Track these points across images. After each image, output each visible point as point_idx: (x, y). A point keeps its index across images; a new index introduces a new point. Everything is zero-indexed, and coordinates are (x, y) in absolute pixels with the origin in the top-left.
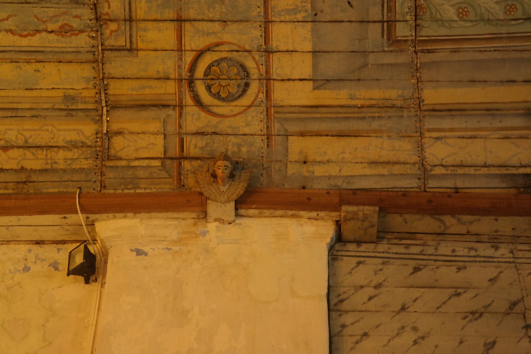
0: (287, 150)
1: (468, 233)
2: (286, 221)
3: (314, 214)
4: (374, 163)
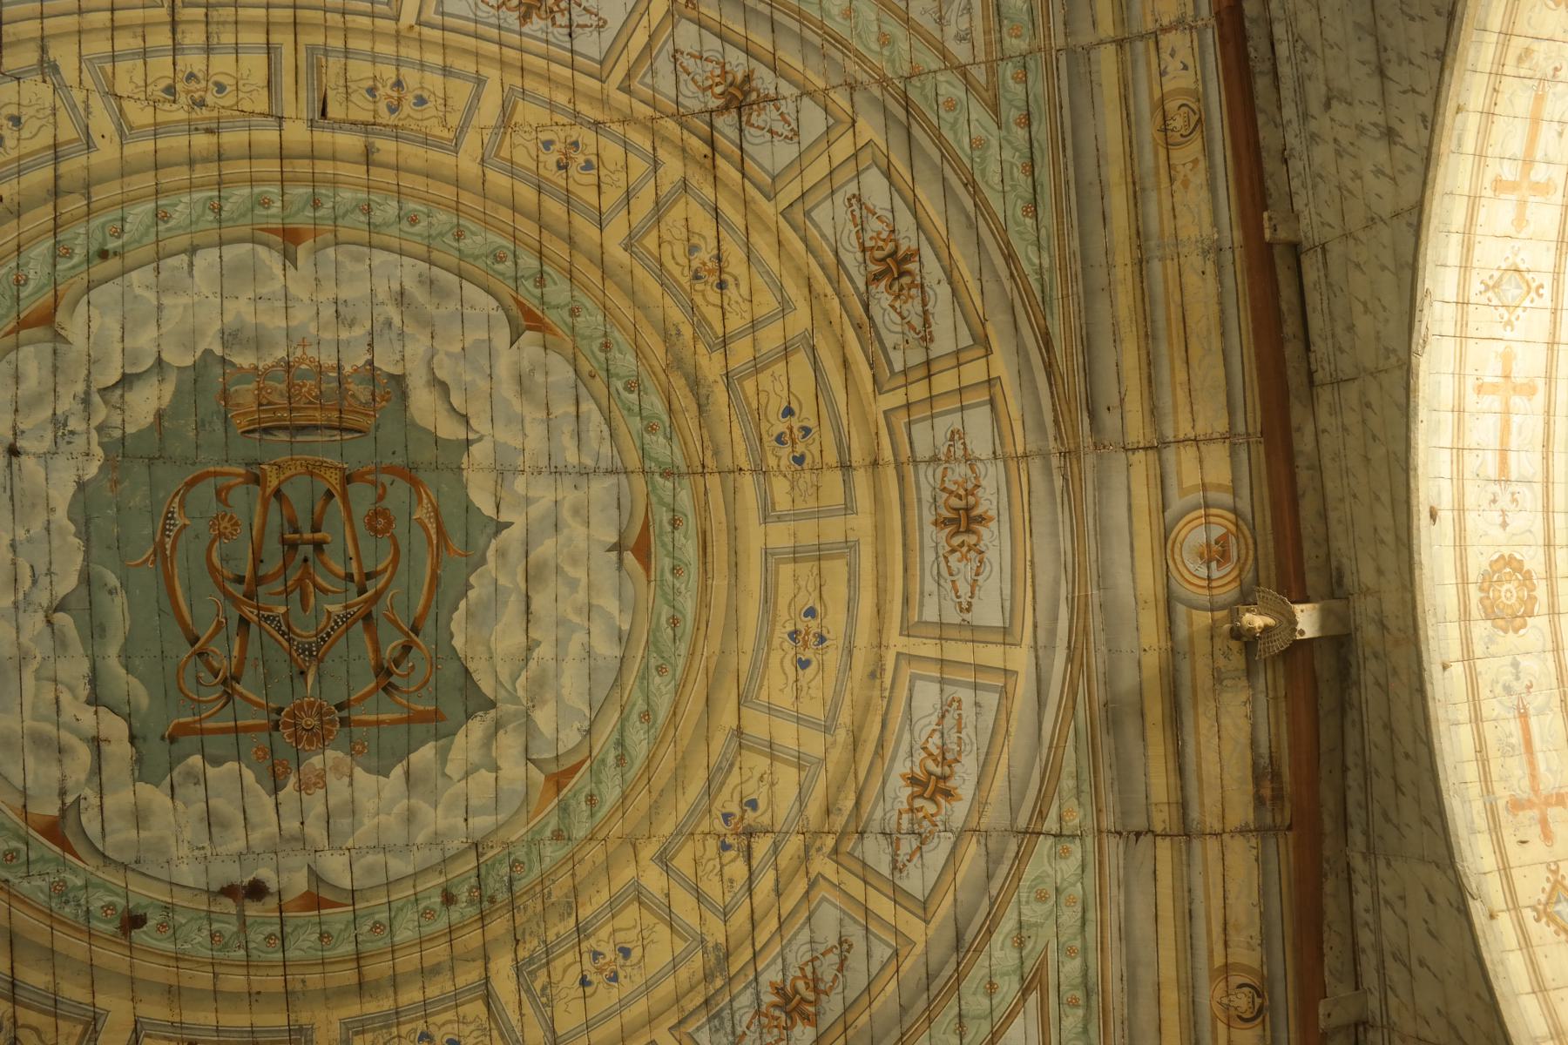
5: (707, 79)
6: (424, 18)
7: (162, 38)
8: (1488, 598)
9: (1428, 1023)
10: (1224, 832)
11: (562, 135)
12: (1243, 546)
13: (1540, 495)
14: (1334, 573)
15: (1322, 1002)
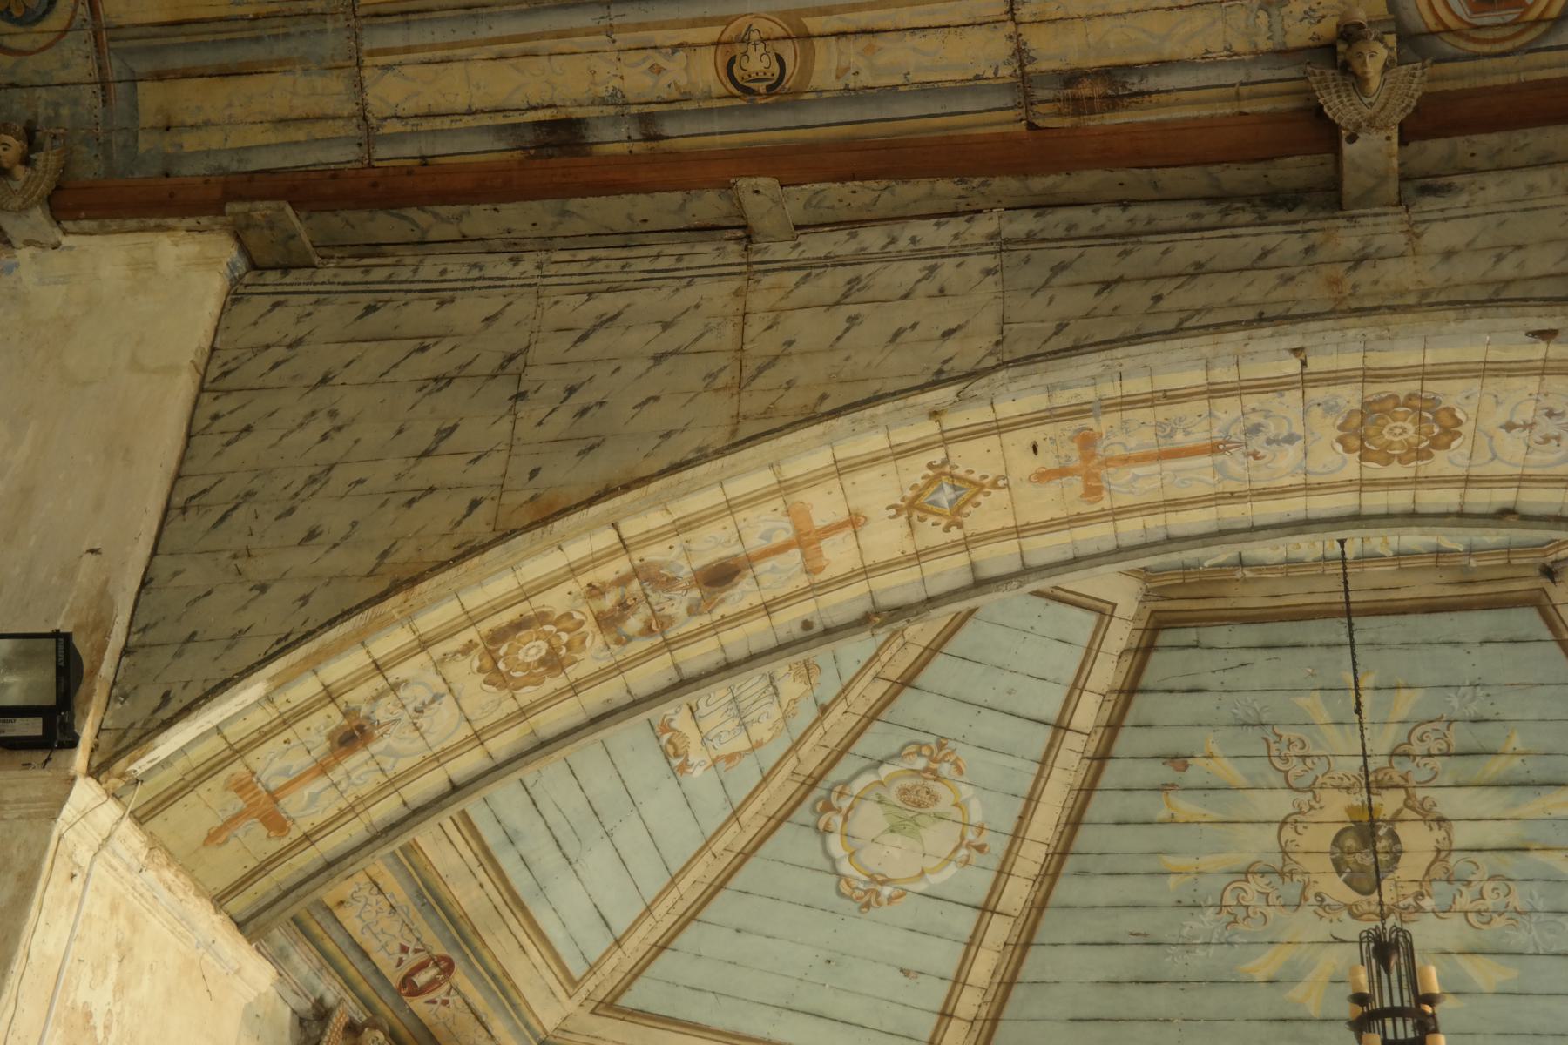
0: (135, 106)
1: (465, 238)
2: (147, 237)
3: (190, 222)
4: (282, 122)
8: (1397, 405)
9: (769, 328)
10: (1017, 24)
12: (1499, 33)
13: (1549, 471)
14: (1441, 181)
15: (775, 182)
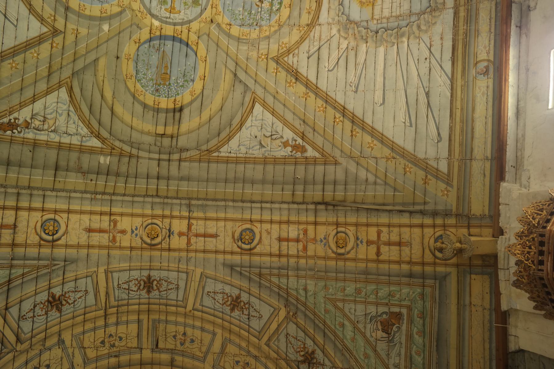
5: (298, 348)
6: (195, 307)
7: (101, 322)
11: (243, 359)
